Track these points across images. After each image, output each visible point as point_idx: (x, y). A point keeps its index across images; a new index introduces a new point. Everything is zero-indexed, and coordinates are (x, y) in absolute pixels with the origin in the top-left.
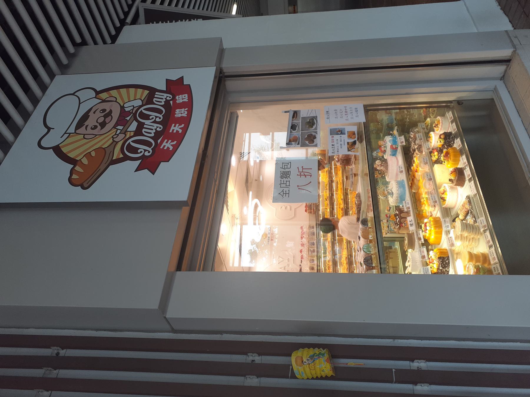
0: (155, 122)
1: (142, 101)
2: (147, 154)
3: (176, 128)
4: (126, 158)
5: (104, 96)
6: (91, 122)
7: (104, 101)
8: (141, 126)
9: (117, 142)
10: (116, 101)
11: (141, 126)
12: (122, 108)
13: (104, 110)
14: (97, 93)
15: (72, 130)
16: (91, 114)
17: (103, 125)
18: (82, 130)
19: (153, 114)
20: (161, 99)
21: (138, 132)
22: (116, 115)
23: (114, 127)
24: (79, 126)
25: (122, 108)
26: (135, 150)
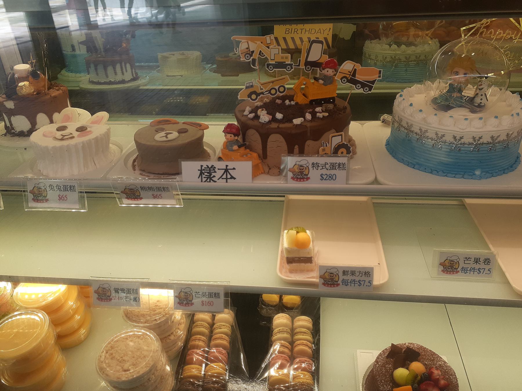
3: (299, 180)
4: (293, 174)
5: (307, 168)
7: (306, 168)
8: (300, 175)
11: (300, 175)
12: (304, 171)
13: (303, 169)
18: (299, 167)
19: (302, 176)
20: (306, 177)
21: (298, 175)
22: (303, 171)
24: (300, 166)
25: (304, 171)
26: (295, 175)
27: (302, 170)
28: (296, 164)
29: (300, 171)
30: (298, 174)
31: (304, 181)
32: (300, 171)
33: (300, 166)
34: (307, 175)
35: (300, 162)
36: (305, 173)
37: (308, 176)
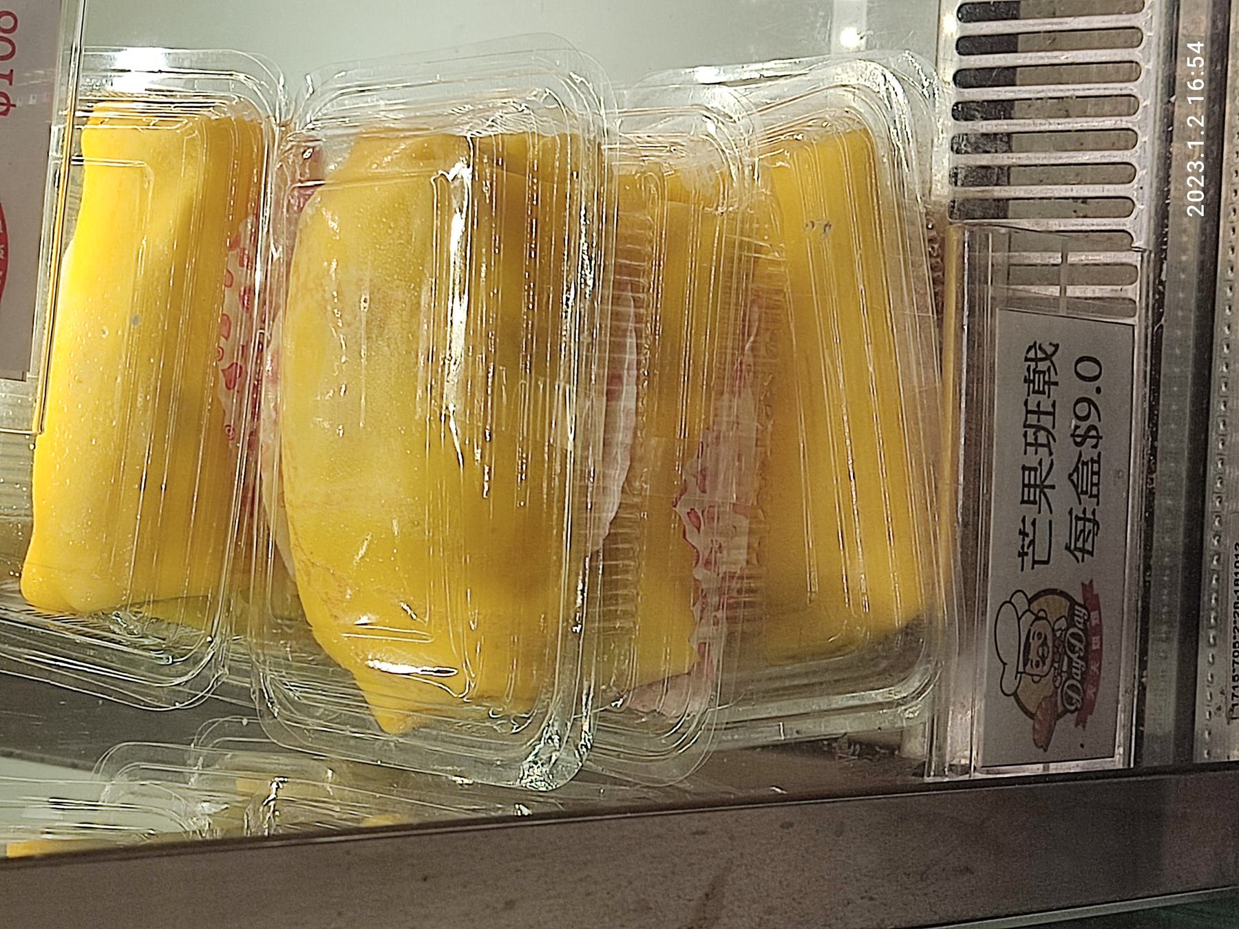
0: (1079, 657)
1: (1067, 620)
2: (1079, 706)
4: (1066, 711)
5: (1035, 606)
6: (1033, 656)
7: (1038, 618)
8: (1070, 659)
9: (1057, 688)
10: (1046, 619)
11: (1070, 659)
14: (1030, 601)
15: (1021, 670)
16: (1031, 640)
17: (1043, 658)
23: (1052, 666)
25: (1053, 630)
27: (1044, 644)
28: (1015, 694)
29: (1048, 661)
30: (1065, 675)
31: (1098, 630)
32: (1048, 661)
33: (1025, 665)
34: (1073, 602)
35: (1005, 664)
36: (1063, 623)
37: (1080, 600)
